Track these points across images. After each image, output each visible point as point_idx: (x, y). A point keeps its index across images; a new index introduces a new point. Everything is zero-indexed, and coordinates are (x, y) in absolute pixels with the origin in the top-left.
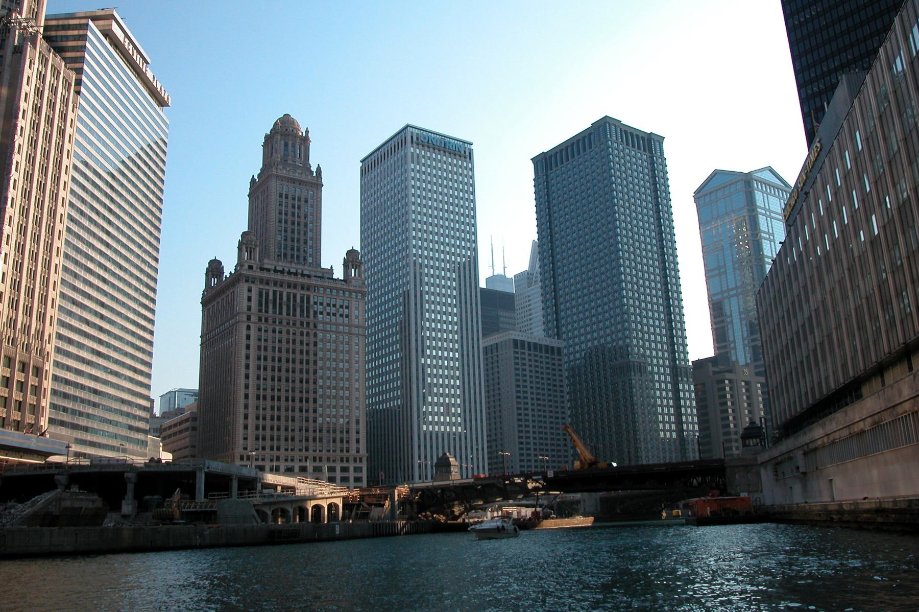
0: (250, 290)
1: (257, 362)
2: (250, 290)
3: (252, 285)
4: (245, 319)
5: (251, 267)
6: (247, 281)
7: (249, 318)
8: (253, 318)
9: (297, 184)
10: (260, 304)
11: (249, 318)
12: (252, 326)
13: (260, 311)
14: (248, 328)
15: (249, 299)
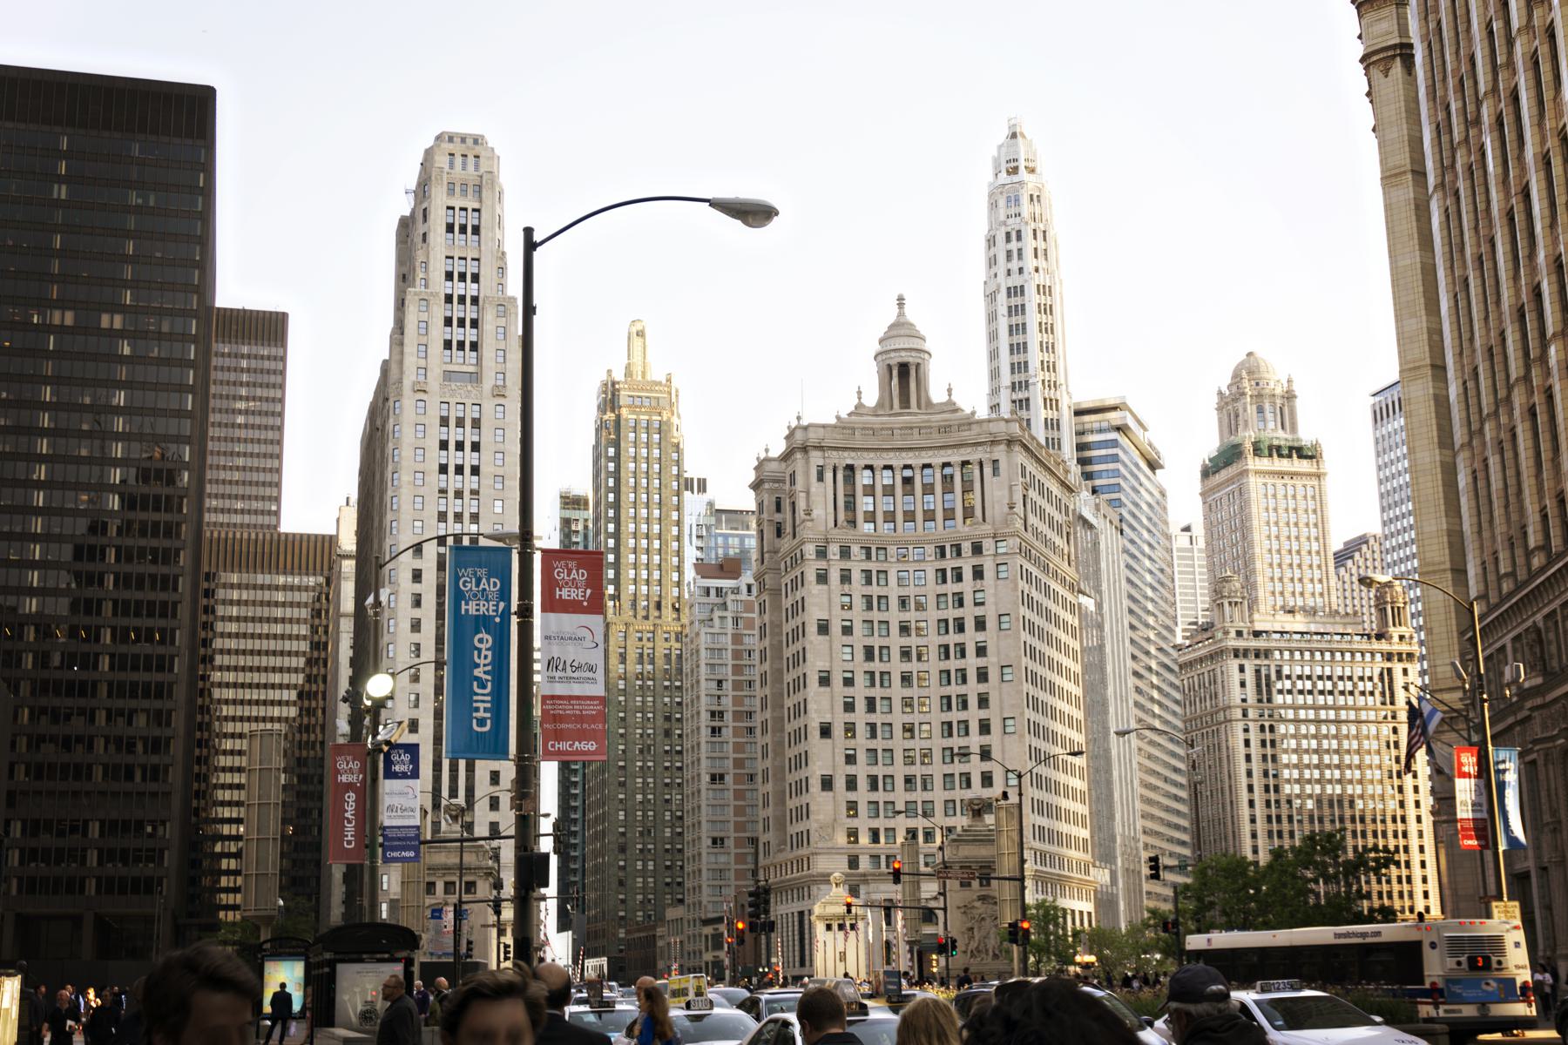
0: (1242, 669)
1: (1264, 781)
2: (1242, 669)
3: (1244, 662)
4: (1240, 716)
5: (1239, 634)
6: (1236, 656)
7: (1245, 715)
8: (1252, 714)
9: (1287, 480)
10: (1259, 691)
11: (1245, 715)
12: (1251, 724)
13: (1260, 701)
14: (1246, 730)
15: (1243, 684)
